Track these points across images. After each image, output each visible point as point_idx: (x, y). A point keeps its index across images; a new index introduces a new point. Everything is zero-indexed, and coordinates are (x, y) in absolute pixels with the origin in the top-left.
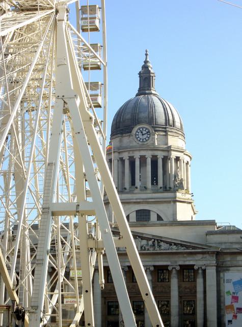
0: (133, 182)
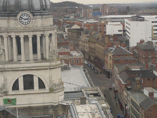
0: (19, 53)
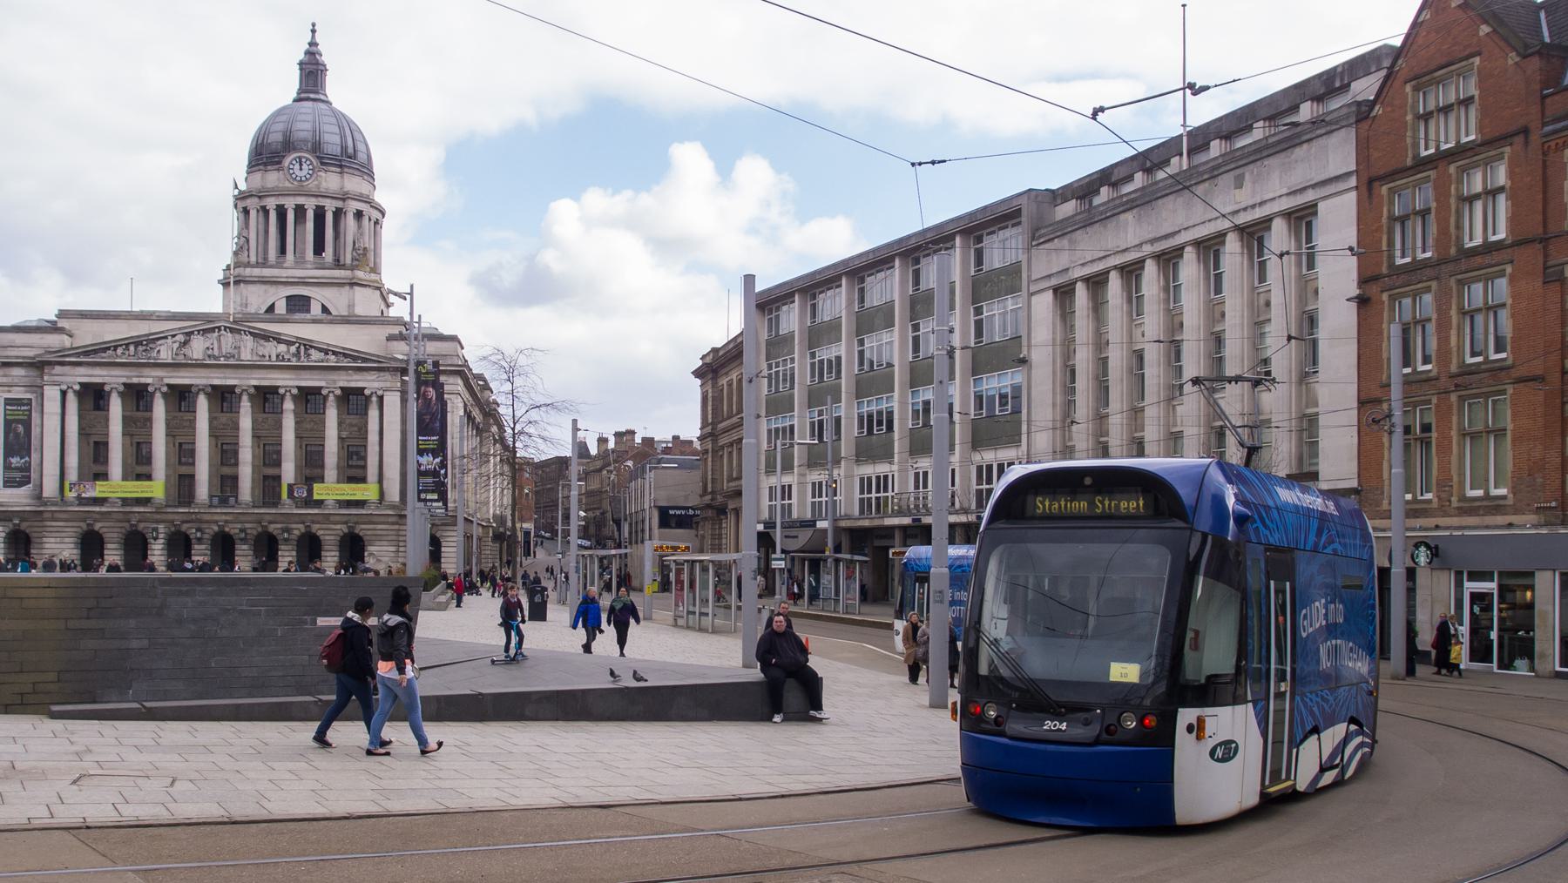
0: (282, 250)
